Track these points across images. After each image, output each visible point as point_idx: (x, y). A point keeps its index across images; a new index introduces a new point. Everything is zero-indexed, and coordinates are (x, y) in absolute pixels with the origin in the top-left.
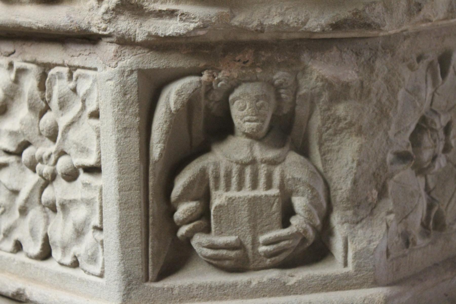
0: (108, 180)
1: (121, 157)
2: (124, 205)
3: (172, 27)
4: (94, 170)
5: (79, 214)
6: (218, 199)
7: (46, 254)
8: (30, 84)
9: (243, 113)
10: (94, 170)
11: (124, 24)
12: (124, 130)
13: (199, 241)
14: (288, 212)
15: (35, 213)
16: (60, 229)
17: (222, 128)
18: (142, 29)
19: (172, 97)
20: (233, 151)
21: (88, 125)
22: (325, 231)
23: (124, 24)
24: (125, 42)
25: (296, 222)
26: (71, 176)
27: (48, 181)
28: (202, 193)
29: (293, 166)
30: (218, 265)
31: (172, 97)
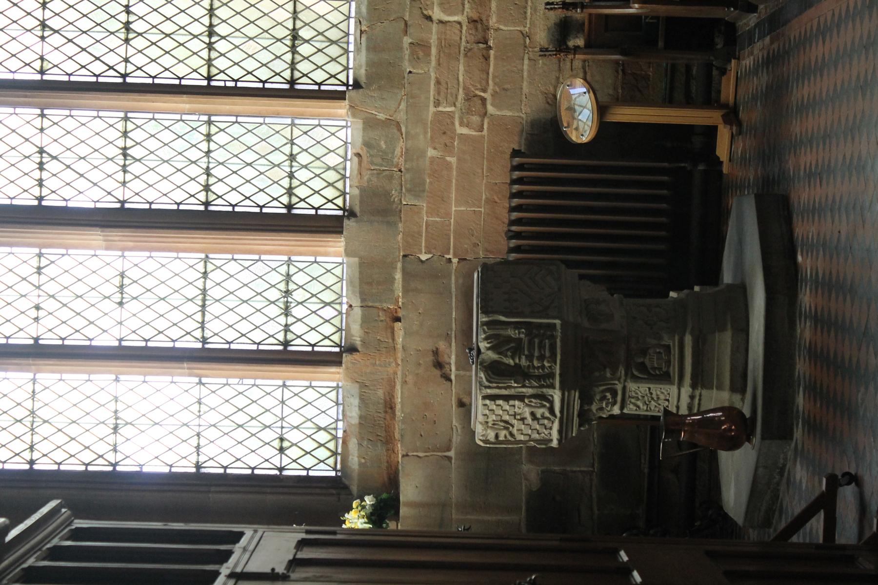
0: (651, 386)
1: (648, 383)
2: (656, 384)
3: (623, 372)
4: (649, 389)
5: (659, 393)
6: (656, 365)
7: (668, 400)
8: (633, 400)
9: (640, 360)
10: (649, 389)
11: (622, 381)
12: (641, 382)
13: (664, 370)
14: (659, 352)
15: (660, 402)
16: (662, 397)
17: (643, 364)
18: (623, 378)
19: (636, 373)
20: (647, 362)
21: (641, 389)
22: (664, 346)
23: (622, 381)
24: (625, 381)
25: (662, 351)
26: (651, 394)
27: (652, 399)
28: (654, 369)
29: (651, 351)
30: (669, 366)
31: (636, 373)
